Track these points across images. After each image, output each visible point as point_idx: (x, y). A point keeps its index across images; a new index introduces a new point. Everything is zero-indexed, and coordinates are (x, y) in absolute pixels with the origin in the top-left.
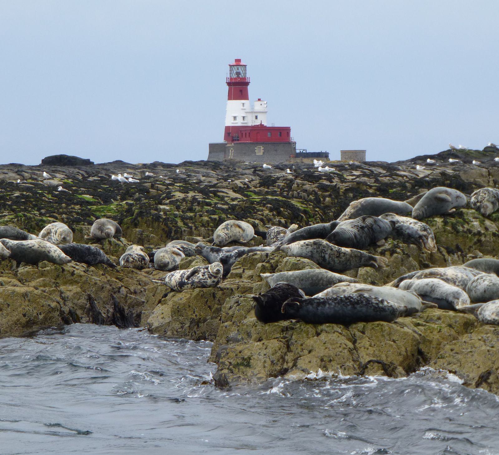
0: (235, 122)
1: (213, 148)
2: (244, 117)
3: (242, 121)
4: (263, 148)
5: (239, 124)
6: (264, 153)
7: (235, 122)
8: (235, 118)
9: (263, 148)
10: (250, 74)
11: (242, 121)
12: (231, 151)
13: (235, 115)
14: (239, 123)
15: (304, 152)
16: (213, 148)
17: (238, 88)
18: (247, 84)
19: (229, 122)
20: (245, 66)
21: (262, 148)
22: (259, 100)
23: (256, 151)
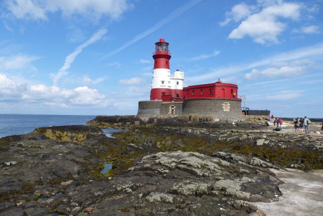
0: (163, 85)
1: (142, 105)
2: (169, 82)
6: (230, 109)
7: (163, 85)
8: (163, 82)
10: (172, 51)
12: (170, 108)
13: (163, 80)
14: (166, 86)
16: (142, 105)
19: (157, 85)
20: (167, 44)
21: (229, 105)
22: (177, 70)
23: (223, 107)
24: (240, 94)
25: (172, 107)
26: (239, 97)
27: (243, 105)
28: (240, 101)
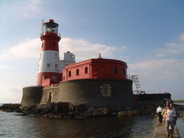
2: (56, 65)
3: (55, 69)
4: (111, 87)
5: (53, 71)
6: (111, 93)
8: (48, 65)
9: (111, 87)
10: (60, 31)
11: (55, 69)
12: (49, 94)
13: (48, 63)
15: (142, 93)
17: (51, 41)
18: (59, 39)
20: (56, 25)
21: (109, 87)
23: (101, 91)
24: (130, 73)
25: (51, 93)
26: (128, 78)
27: (134, 88)
28: (130, 82)
